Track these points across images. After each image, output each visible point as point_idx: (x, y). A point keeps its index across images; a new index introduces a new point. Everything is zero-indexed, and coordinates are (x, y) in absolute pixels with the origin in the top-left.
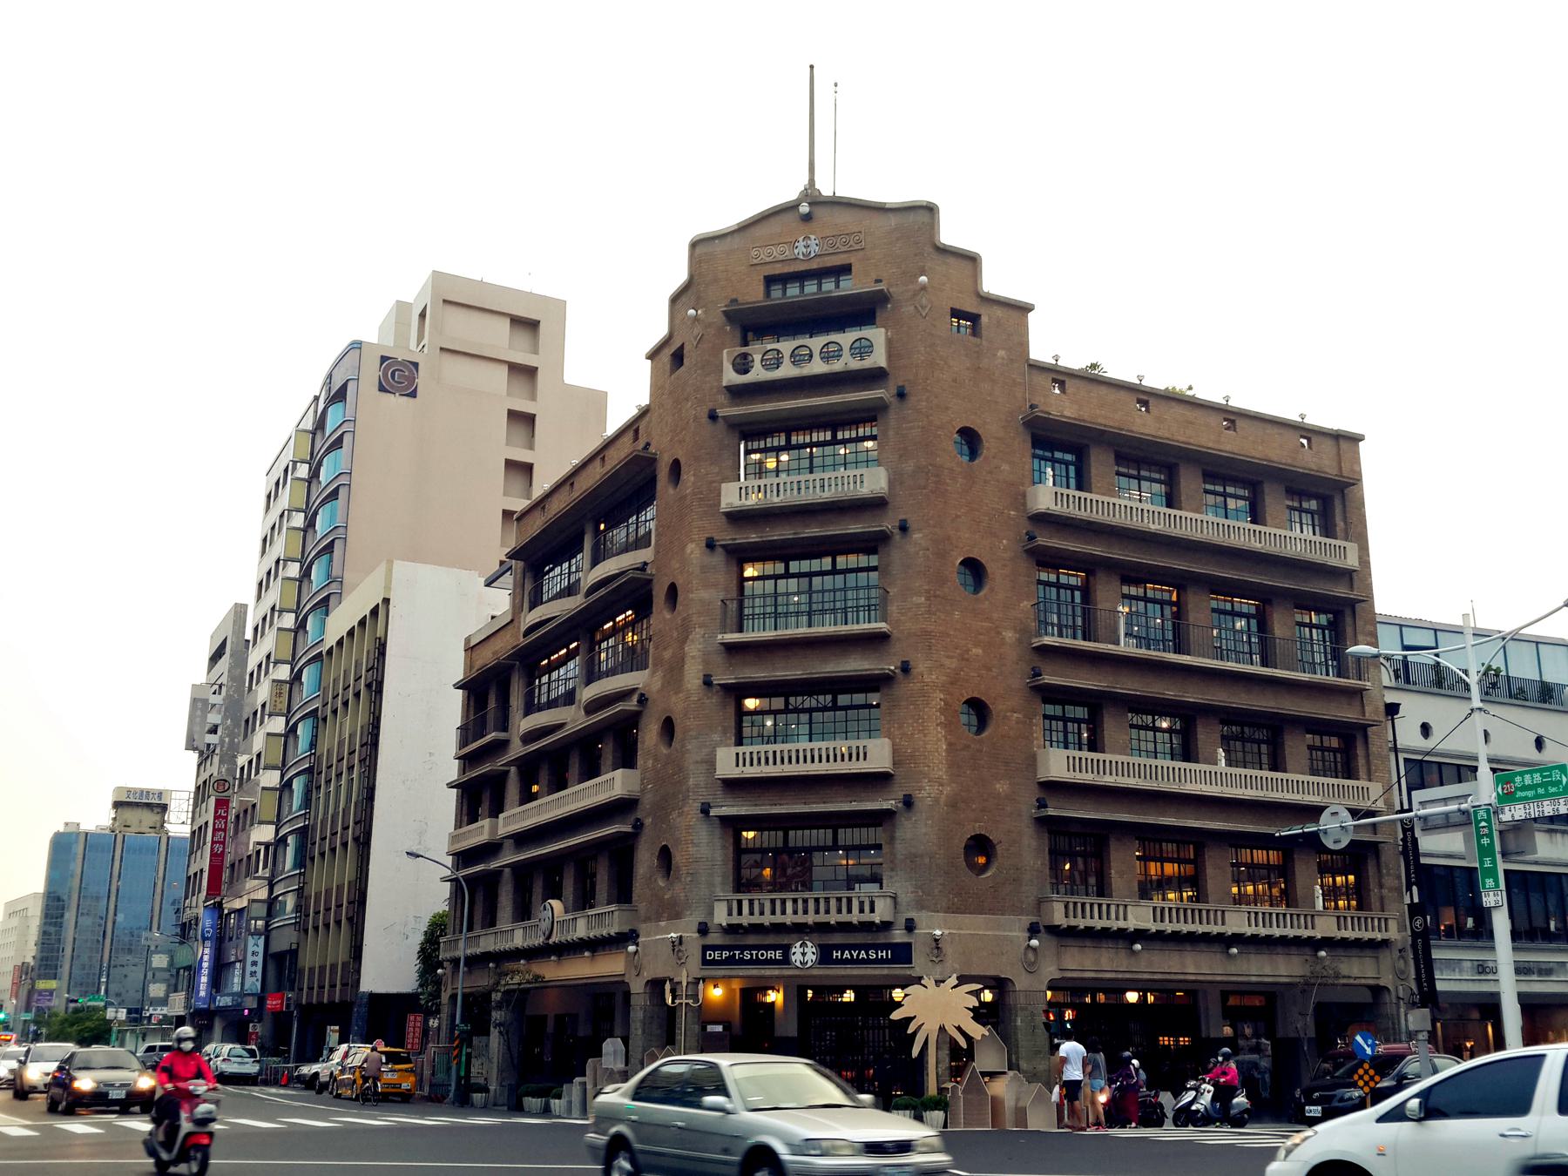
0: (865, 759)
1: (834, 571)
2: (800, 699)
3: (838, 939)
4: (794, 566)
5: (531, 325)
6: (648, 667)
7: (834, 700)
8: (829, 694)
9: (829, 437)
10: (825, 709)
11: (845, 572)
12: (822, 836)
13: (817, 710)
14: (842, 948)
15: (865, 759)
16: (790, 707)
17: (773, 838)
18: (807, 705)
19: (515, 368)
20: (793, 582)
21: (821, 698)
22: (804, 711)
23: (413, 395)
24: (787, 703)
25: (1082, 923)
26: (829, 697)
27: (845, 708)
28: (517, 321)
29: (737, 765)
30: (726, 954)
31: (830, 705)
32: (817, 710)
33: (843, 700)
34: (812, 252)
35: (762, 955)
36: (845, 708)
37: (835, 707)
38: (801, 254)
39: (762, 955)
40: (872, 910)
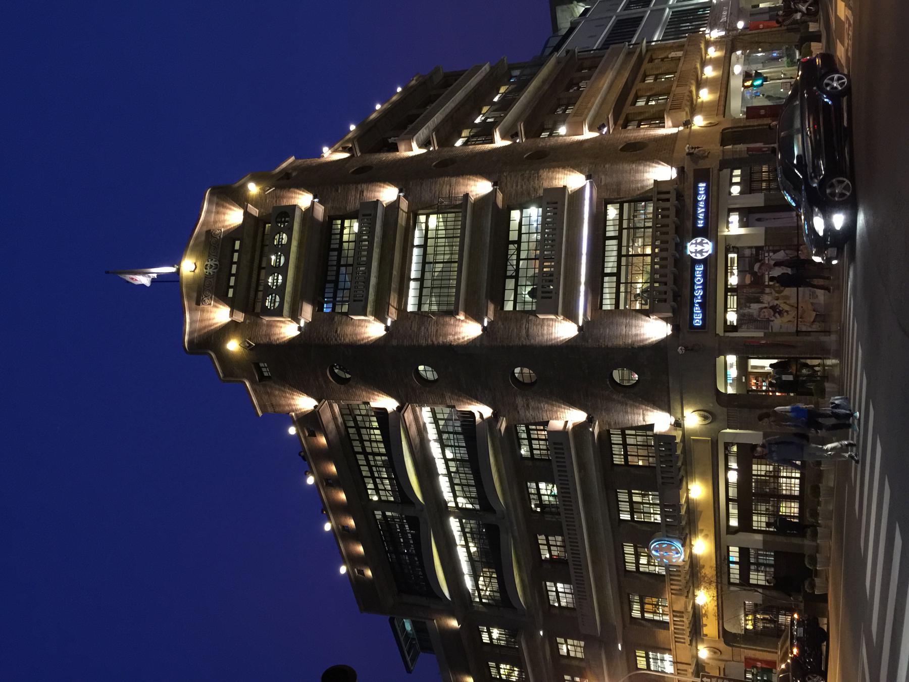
0: (556, 203)
2: (509, 268)
3: (689, 224)
6: (472, 414)
8: (508, 247)
9: (336, 253)
10: (519, 250)
14: (696, 218)
15: (556, 203)
16: (514, 274)
17: (609, 284)
18: (515, 262)
21: (510, 252)
24: (511, 277)
26: (511, 246)
27: (520, 234)
29: (551, 298)
30: (697, 309)
31: (516, 245)
32: (518, 255)
33: (513, 236)
34: (216, 263)
35: (699, 281)
36: (520, 234)
37: (519, 242)
38: (214, 270)
39: (699, 281)
40: (668, 193)
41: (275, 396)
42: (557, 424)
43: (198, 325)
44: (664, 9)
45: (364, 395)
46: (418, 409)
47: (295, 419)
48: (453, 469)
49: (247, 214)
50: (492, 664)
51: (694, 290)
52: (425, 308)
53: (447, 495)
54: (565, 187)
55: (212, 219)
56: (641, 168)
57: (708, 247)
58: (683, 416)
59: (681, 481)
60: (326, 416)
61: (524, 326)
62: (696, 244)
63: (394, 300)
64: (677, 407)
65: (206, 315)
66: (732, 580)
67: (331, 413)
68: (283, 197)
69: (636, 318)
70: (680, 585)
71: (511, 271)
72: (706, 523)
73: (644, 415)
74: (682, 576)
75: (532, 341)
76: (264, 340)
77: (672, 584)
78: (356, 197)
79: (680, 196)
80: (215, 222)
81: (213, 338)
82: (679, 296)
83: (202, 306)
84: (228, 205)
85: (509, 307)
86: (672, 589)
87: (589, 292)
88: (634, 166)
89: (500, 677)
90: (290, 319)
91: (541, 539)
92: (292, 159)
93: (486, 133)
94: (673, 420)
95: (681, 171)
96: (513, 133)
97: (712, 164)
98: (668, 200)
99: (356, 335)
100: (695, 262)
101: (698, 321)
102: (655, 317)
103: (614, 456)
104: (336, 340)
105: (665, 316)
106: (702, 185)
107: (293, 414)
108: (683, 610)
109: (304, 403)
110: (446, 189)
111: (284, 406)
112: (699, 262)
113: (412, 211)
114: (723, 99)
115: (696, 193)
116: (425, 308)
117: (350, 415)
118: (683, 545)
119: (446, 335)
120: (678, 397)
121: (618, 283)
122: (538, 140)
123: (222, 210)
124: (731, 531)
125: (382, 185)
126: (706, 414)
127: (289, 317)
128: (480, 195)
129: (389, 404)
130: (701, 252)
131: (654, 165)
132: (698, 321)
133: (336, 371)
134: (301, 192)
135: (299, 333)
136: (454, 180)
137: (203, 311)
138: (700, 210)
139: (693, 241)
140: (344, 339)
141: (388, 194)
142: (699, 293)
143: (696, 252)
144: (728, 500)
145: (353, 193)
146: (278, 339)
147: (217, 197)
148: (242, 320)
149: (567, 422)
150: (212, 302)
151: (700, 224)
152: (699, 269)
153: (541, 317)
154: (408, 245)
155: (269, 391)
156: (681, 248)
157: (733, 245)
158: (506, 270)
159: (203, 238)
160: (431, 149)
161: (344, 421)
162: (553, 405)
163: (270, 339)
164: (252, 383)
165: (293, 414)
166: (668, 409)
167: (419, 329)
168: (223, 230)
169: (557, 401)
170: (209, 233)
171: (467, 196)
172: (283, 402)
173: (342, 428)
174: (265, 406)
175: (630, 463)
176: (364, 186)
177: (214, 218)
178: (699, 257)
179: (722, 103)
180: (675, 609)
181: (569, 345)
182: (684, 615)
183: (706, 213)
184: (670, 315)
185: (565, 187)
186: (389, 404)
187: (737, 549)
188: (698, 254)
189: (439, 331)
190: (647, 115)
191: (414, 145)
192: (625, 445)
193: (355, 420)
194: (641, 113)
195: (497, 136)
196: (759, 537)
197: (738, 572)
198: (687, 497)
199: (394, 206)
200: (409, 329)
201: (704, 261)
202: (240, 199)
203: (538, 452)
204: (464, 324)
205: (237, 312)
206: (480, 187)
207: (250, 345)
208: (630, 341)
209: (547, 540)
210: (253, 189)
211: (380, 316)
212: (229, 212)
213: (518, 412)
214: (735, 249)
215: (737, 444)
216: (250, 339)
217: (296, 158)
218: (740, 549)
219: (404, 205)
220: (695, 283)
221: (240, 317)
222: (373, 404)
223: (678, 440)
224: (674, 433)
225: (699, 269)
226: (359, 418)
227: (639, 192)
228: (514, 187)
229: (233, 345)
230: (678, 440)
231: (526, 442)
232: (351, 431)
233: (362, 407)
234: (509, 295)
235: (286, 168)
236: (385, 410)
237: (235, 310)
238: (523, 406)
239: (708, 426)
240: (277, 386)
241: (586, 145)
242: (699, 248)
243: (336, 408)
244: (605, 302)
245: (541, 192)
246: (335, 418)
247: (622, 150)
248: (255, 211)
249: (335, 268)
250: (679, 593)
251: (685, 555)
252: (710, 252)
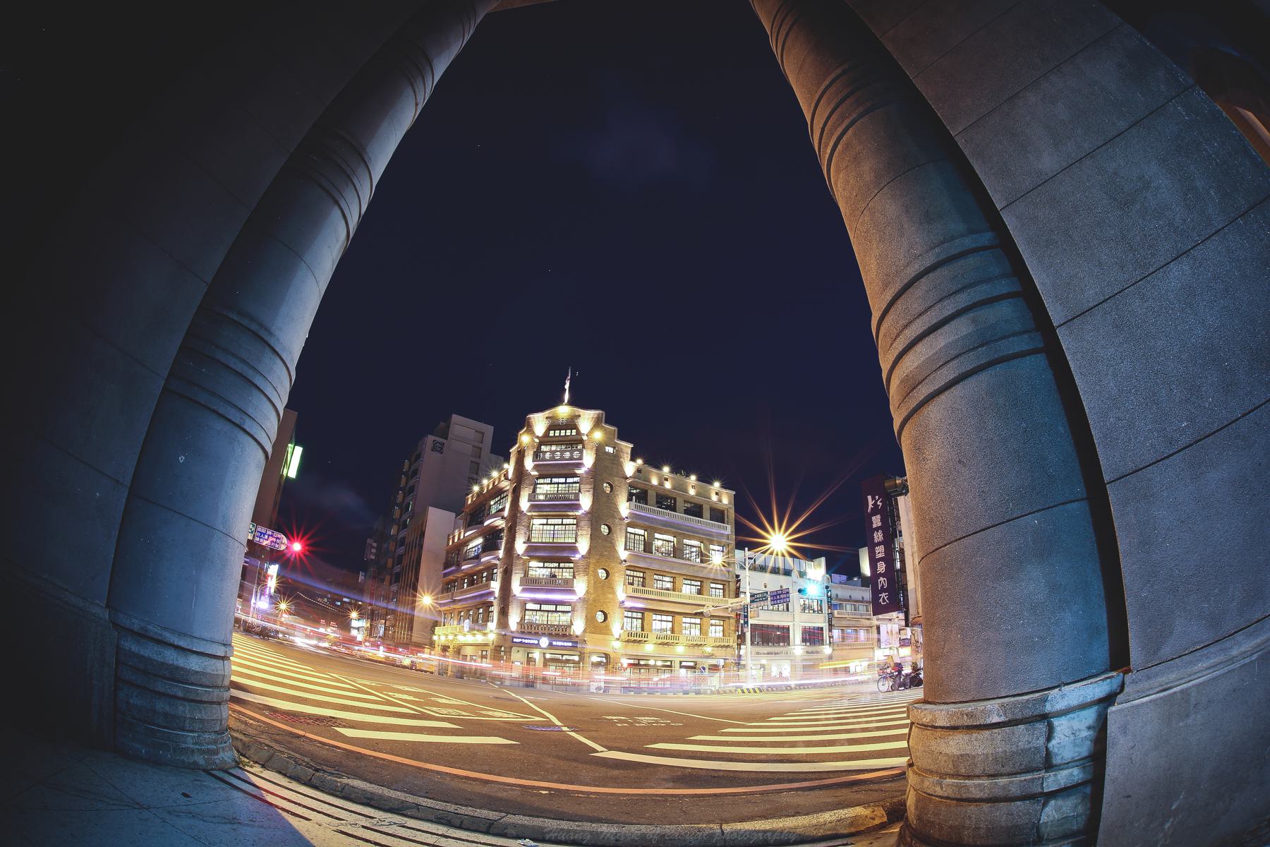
1: (562, 524)
3: (554, 638)
4: (550, 521)
5: (483, 433)
6: (498, 549)
7: (559, 565)
10: (556, 568)
11: (566, 525)
12: (552, 608)
13: (553, 568)
17: (537, 607)
19: (474, 446)
20: (549, 527)
23: (442, 453)
25: (633, 638)
26: (557, 564)
27: (563, 568)
28: (476, 431)
30: (520, 640)
33: (562, 565)
36: (563, 568)
37: (559, 568)
43: (536, 420)
65: (541, 423)
67: (505, 485)
71: (546, 565)
76: (526, 454)
79: (564, 636)
94: (494, 630)
106: (570, 644)
110: (584, 532)
121: (537, 611)
129: (506, 513)
151: (554, 643)
152: (536, 642)
154: (562, 517)
156: (544, 634)
158: (547, 562)
164: (518, 448)
167: (523, 526)
170: (580, 416)
176: (592, 492)
191: (629, 511)
199: (577, 507)
201: (538, 644)
211: (533, 508)
219: (577, 513)
221: (537, 440)
243: (508, 487)
246: (506, 486)
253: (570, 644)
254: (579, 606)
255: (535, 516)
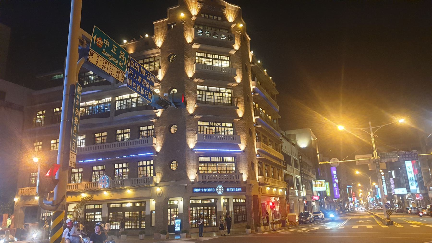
10: (219, 126)
13: (217, 126)
14: (230, 188)
17: (208, 159)
18: (214, 125)
21: (218, 123)
22: (214, 126)
24: (209, 124)
26: (220, 124)
30: (199, 190)
32: (217, 126)
33: (224, 124)
35: (209, 190)
36: (224, 127)
39: (209, 190)
40: (239, 179)
41: (162, 30)
42: (155, 140)
44: (294, 173)
45: (163, 67)
46: (158, 88)
47: (152, 38)
48: (133, 100)
49: (232, 23)
50: (44, 112)
51: (206, 188)
52: (198, 92)
53: (120, 97)
54: (241, 143)
55: (230, 9)
56: (246, 169)
57: (220, 192)
58: (159, 187)
59: (134, 187)
60: (154, 51)
61: (192, 129)
62: (221, 188)
63: (201, 81)
64: (163, 184)
65: (194, 4)
66: (87, 206)
68: (237, 37)
69: (196, 168)
70: (89, 187)
71: (212, 124)
72: (115, 196)
73: (160, 172)
74: (93, 188)
75: (187, 132)
76: (185, 29)
77: (90, 184)
78: (237, 66)
79: (237, 182)
80: (228, 10)
81: (185, 7)
82: (204, 183)
83: (197, 3)
84: (235, 15)
85: (199, 123)
86: (87, 184)
87: (205, 152)
88: (247, 166)
89: (38, 116)
90: (193, 39)
91: (105, 134)
92: (250, 40)
93: (257, 113)
95: (245, 182)
96: (258, 123)
97: (247, 193)
98: (236, 178)
99: (188, 65)
100: (215, 188)
101: (196, 190)
102: (197, 175)
103: (142, 162)
104: (186, 58)
105: (197, 179)
106: (240, 189)
107: (154, 37)
108: (79, 188)
109: (159, 42)
110: (239, 100)
111: (158, 33)
112: (216, 190)
113: (232, 88)
114: (266, 195)
115: (238, 188)
116: (198, 92)
117: (154, 60)
118: (107, 188)
119: (189, 100)
120: (167, 185)
121: (208, 162)
122: (255, 132)
123: (233, 13)
124: (108, 205)
125: (242, 76)
126: (161, 195)
127: (194, 39)
128: (238, 113)
129: (160, 77)
130: (219, 190)
131: (247, 173)
132: (196, 190)
133: (173, 56)
134: (239, 45)
135: (188, 42)
136: (243, 103)
137: (195, 3)
138: (232, 190)
139: (222, 188)
140: (186, 61)
141: (238, 79)
142: (205, 190)
143: (219, 189)
144: (121, 203)
145: (239, 65)
146: (185, 34)
147: (238, 11)
148: (192, 19)
149: (156, 144)
150: (199, 7)
151: (228, 190)
152: (213, 190)
153: (196, 135)
155: (164, 28)
156: (220, 183)
157: (217, 201)
158: (212, 122)
159: (223, 5)
160: (253, 93)
161: (152, 57)
162: (162, 139)
163: (185, 31)
164: (167, 21)
165: (154, 37)
166: (161, 181)
168: (226, 13)
169: (164, 141)
171: (238, 108)
172: (159, 33)
173: (149, 56)
174: (157, 25)
175: (139, 168)
177: (230, 10)
178: (217, 190)
179: (265, 195)
180: (79, 185)
181: (186, 145)
182: (76, 189)
183: (232, 192)
184: (198, 180)
185: (241, 143)
186: (160, 77)
187: (101, 207)
188: (218, 189)
189: (190, 97)
190: (262, 169)
191: (254, 87)
192: (147, 166)
193: (152, 62)
194: (262, 167)
195: (257, 117)
196: (107, 215)
197: (91, 208)
198: (127, 189)
199: (235, 82)
200: (191, 86)
201: (216, 191)
202: (237, 21)
203: (142, 133)
204: (193, 107)
205: (196, 18)
206: (240, 113)
207: (183, 23)
208: (188, 167)
209: (104, 136)
210: (241, 26)
212: (233, 15)
213: (159, 126)
214: (216, 202)
215: (145, 206)
216: (185, 22)
217: (250, 41)
218: (102, 208)
219: (235, 85)
220: (208, 188)
221: (194, 19)
222: (160, 71)
223: (150, 185)
224: (153, 183)
225: (213, 190)
226: (153, 64)
227: (238, 168)
228: (241, 125)
229: (182, 15)
230: (150, 185)
231: (146, 129)
232: (148, 60)
233: (158, 65)
234: (203, 123)
235: (247, 37)
236: (158, 75)
237: (196, 17)
238: (161, 128)
239: (156, 195)
240: (166, 32)
241: (253, 149)
242: (220, 190)
244: (201, 158)
245: (238, 134)
246: (153, 54)
247: (252, 162)
248: (232, 26)
249: (212, 57)
250: (86, 187)
251: (103, 189)
252: (219, 193)
253: (240, 189)
254: (242, 157)
255: (200, 83)
